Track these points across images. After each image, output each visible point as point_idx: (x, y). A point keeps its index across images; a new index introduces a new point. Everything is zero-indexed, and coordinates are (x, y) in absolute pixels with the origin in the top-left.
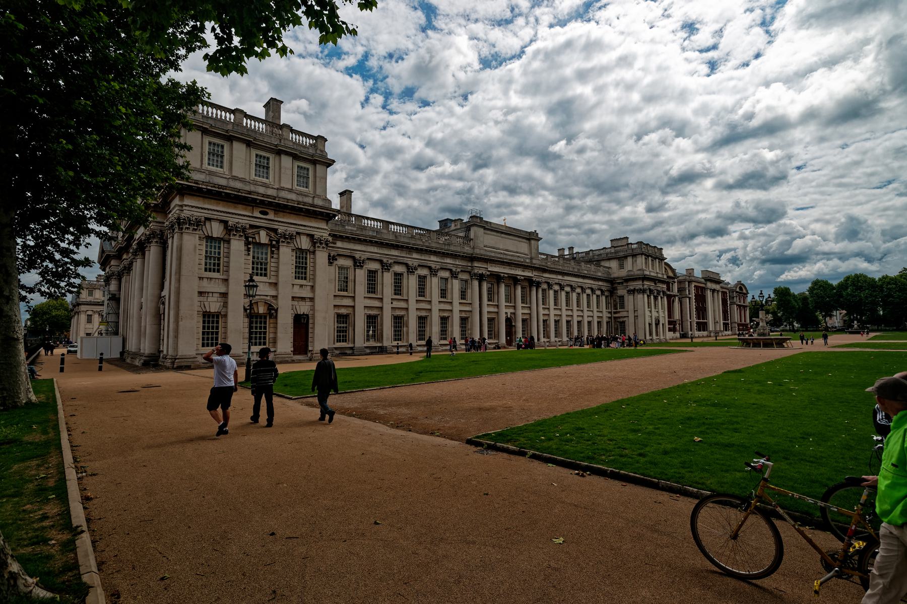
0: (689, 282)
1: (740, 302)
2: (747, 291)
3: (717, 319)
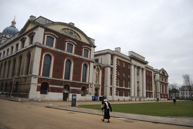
0: (112, 56)
1: (162, 80)
2: (168, 75)
3: (141, 88)
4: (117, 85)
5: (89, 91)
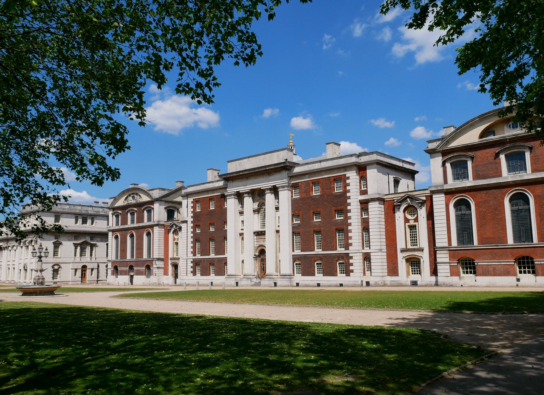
4: (194, 254)
5: (154, 270)
